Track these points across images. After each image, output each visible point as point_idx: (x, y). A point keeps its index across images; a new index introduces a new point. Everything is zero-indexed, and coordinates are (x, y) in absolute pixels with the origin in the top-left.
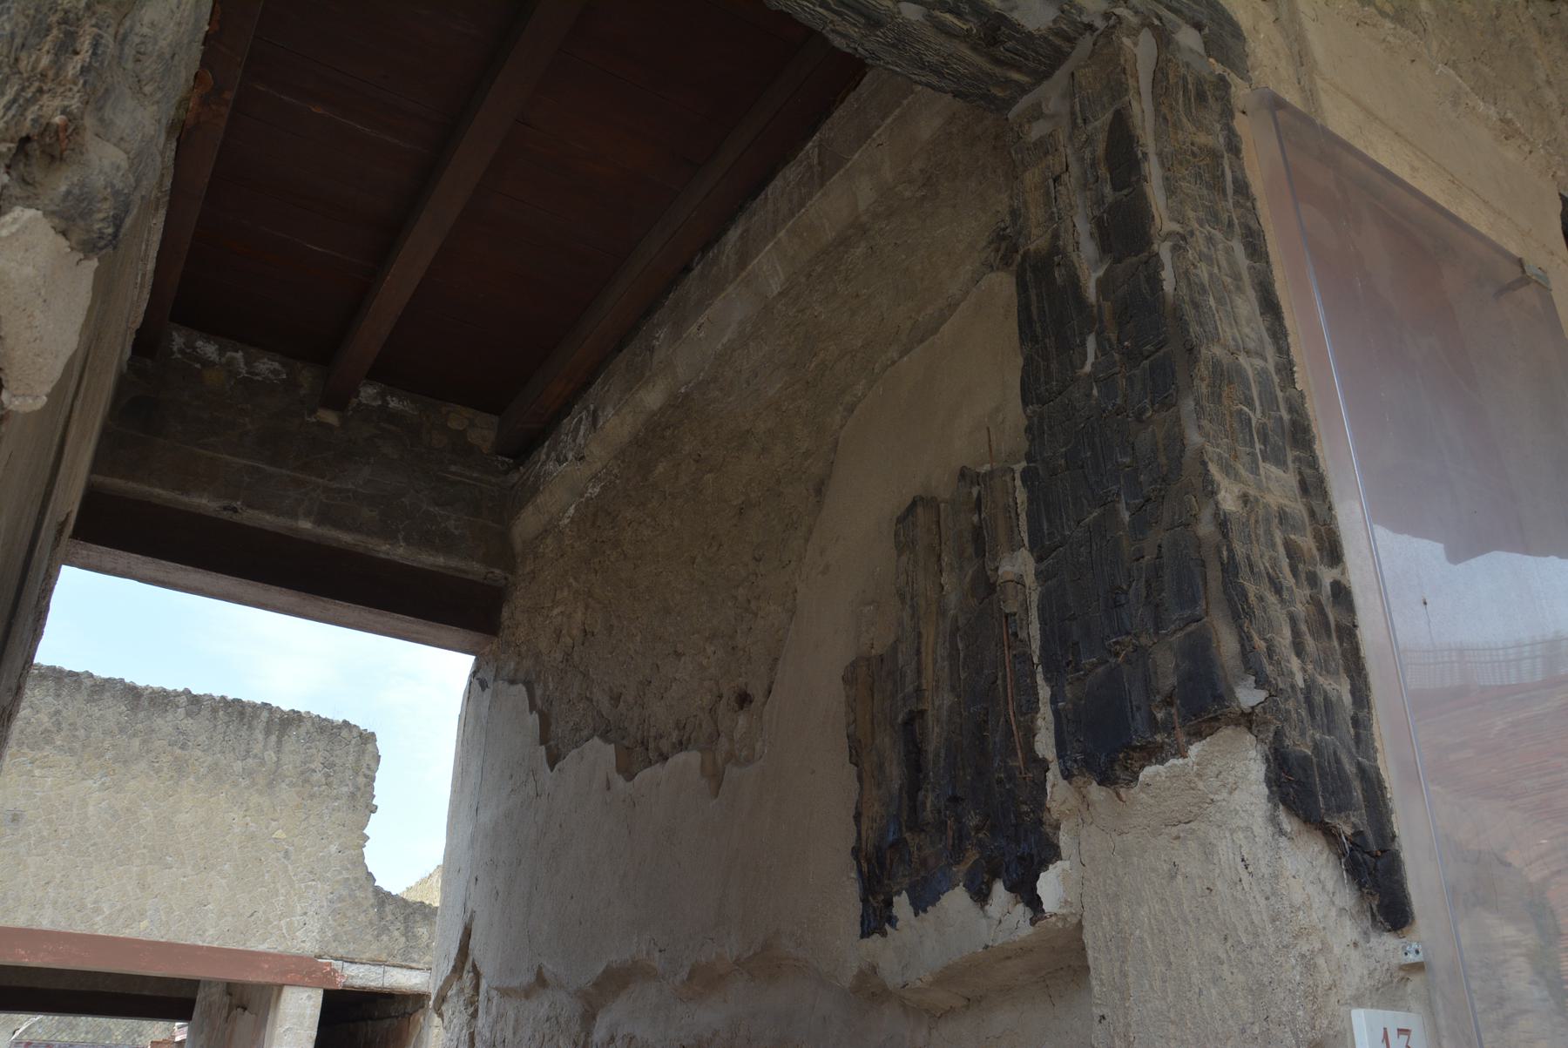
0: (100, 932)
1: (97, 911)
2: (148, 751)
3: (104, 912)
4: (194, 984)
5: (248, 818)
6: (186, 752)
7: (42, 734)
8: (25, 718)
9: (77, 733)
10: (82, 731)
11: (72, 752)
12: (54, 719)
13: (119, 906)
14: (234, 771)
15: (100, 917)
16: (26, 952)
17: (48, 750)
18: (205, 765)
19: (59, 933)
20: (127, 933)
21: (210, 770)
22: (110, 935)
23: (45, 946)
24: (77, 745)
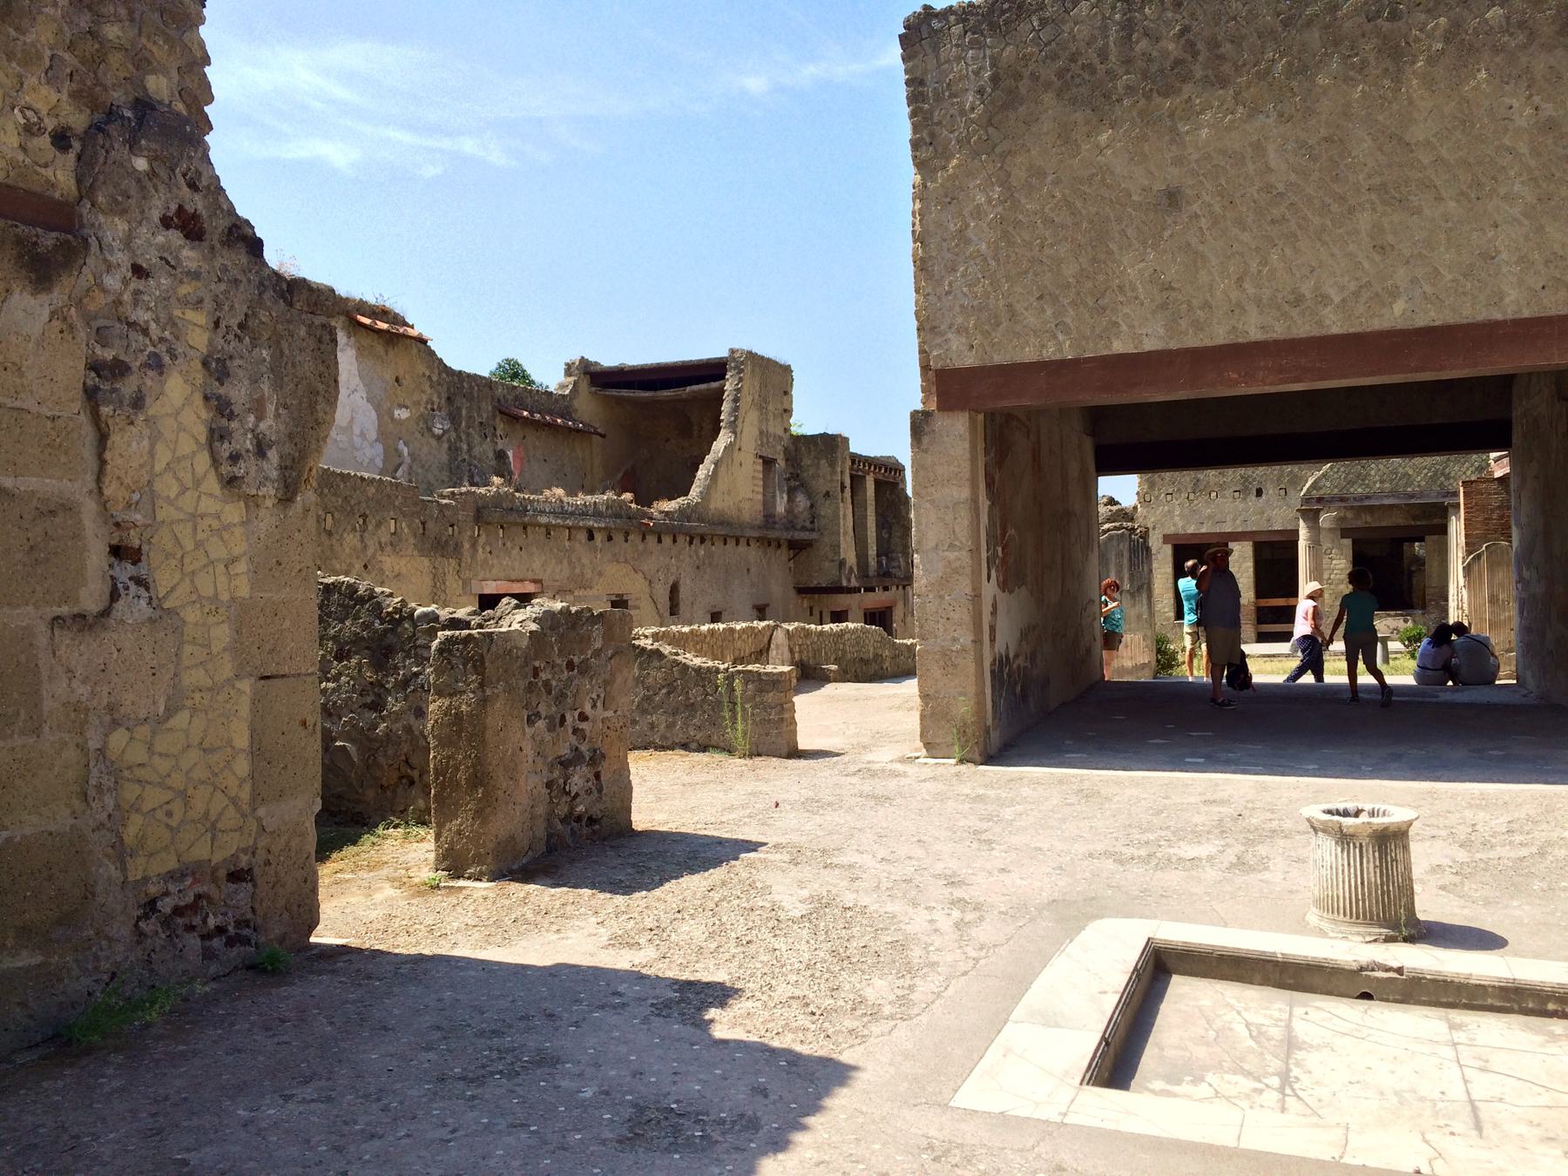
0: (1335, 330)
1: (1324, 299)
2: (1336, 44)
3: (1332, 300)
4: (1504, 384)
5: (1536, 99)
6: (1400, 23)
7: (1172, 69)
8: (1144, 54)
9: (1222, 50)
10: (1228, 45)
11: (1223, 82)
12: (1183, 41)
13: (1353, 286)
14: (1492, 28)
15: (1329, 308)
16: (1239, 374)
17: (1188, 89)
18: (1437, 33)
19: (1276, 342)
20: (1377, 324)
21: (1448, 38)
22: (1351, 331)
23: (1262, 364)
24: (1226, 68)
